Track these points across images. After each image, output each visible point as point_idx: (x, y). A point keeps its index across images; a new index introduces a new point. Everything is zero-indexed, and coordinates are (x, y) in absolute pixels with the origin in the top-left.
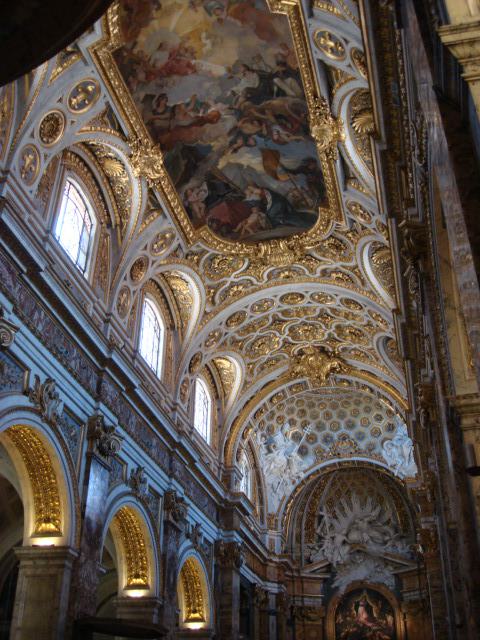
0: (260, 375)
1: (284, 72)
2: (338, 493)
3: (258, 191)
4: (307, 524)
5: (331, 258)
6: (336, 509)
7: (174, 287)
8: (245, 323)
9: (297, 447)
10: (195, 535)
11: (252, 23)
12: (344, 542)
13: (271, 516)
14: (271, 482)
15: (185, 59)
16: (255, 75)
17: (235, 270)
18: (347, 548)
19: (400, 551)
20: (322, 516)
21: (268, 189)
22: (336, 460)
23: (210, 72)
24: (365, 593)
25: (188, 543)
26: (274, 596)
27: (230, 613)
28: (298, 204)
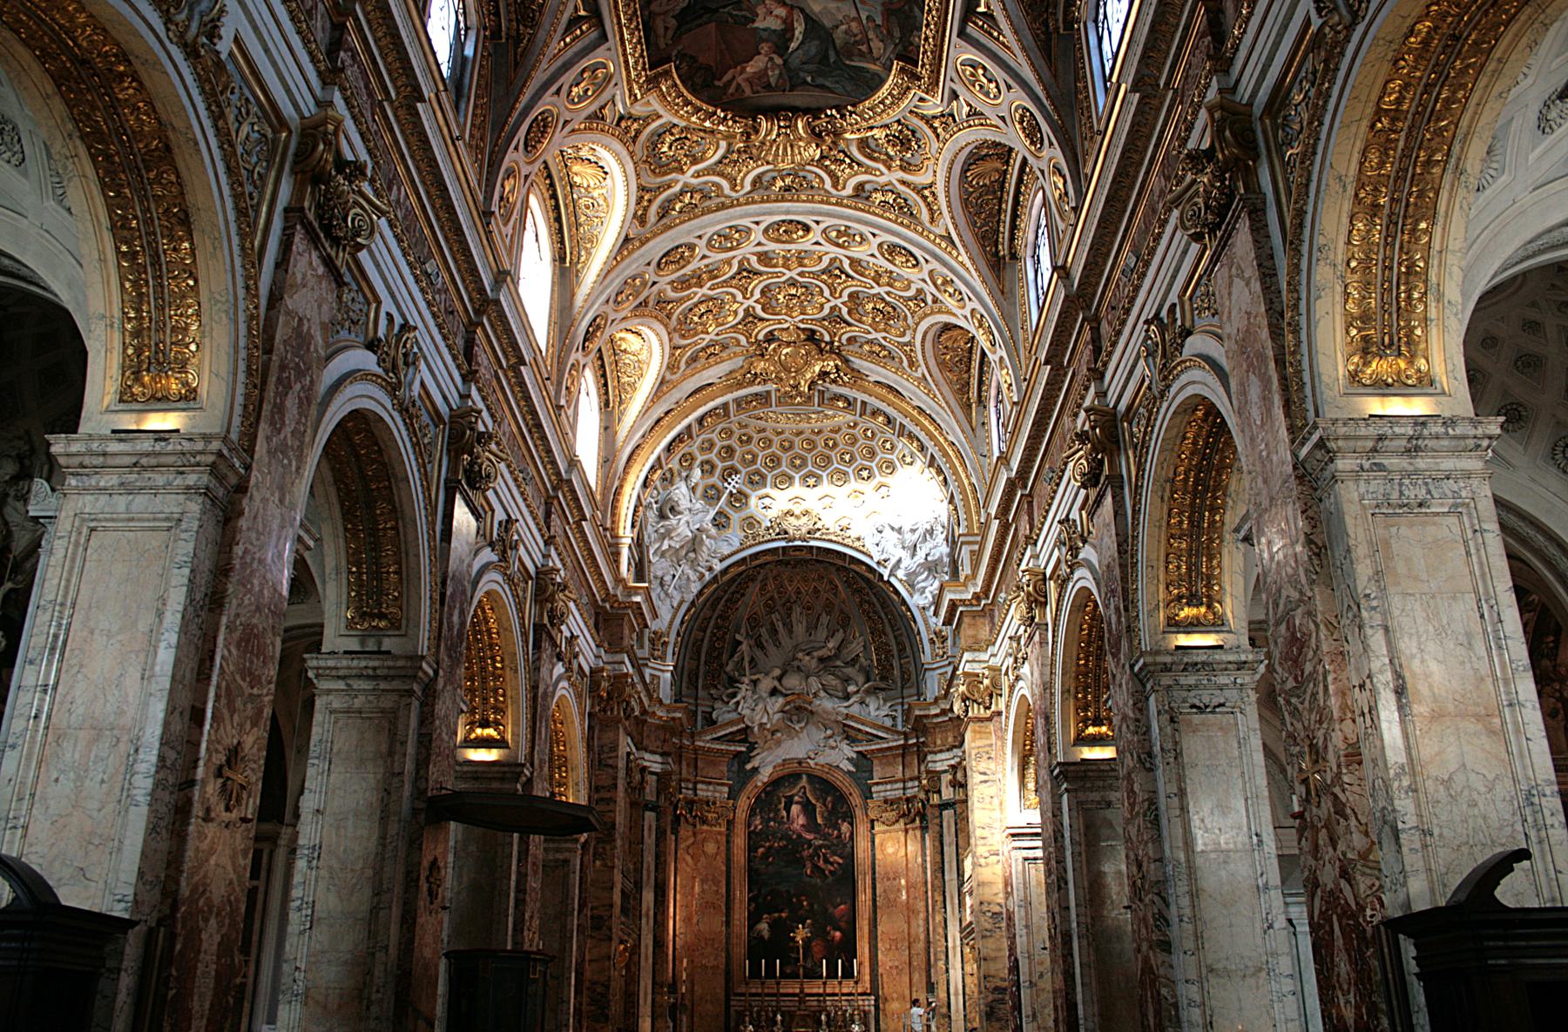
0: (688, 371)
3: (781, 12)
5: (884, 163)
6: (763, 630)
7: (577, 179)
8: (687, 270)
9: (712, 513)
10: (567, 656)
13: (657, 639)
14: (659, 574)
17: (695, 161)
18: (781, 700)
20: (740, 643)
21: (802, 10)
22: (783, 544)
24: (804, 781)
25: (559, 669)
27: (612, 800)
28: (849, 50)
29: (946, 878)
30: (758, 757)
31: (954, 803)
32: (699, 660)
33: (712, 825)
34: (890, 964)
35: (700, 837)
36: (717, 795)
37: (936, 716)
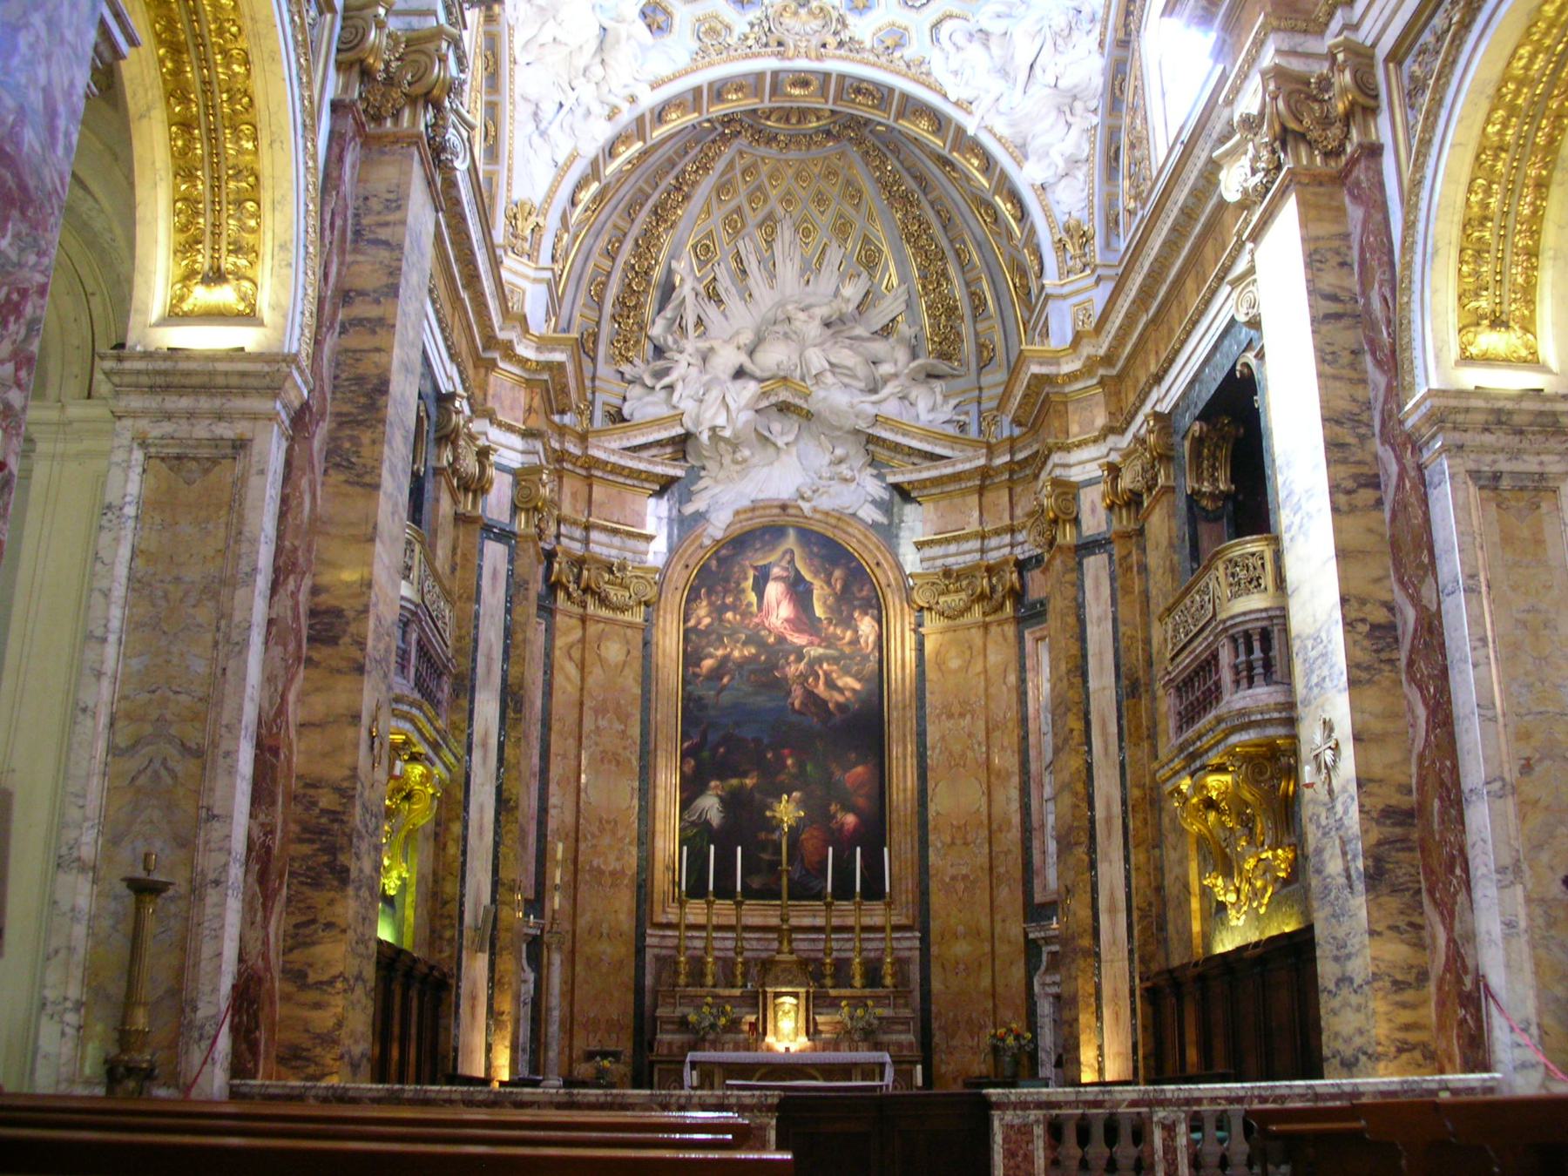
2: (734, 225)
4: (621, 302)
12: (740, 373)
14: (533, 93)
18: (752, 387)
19: (925, 417)
24: (791, 541)
26: (508, 479)
29: (1093, 684)
30: (706, 495)
31: (1109, 541)
32: (600, 305)
33: (615, 608)
34: (952, 871)
35: (593, 629)
36: (629, 555)
37: (1073, 377)
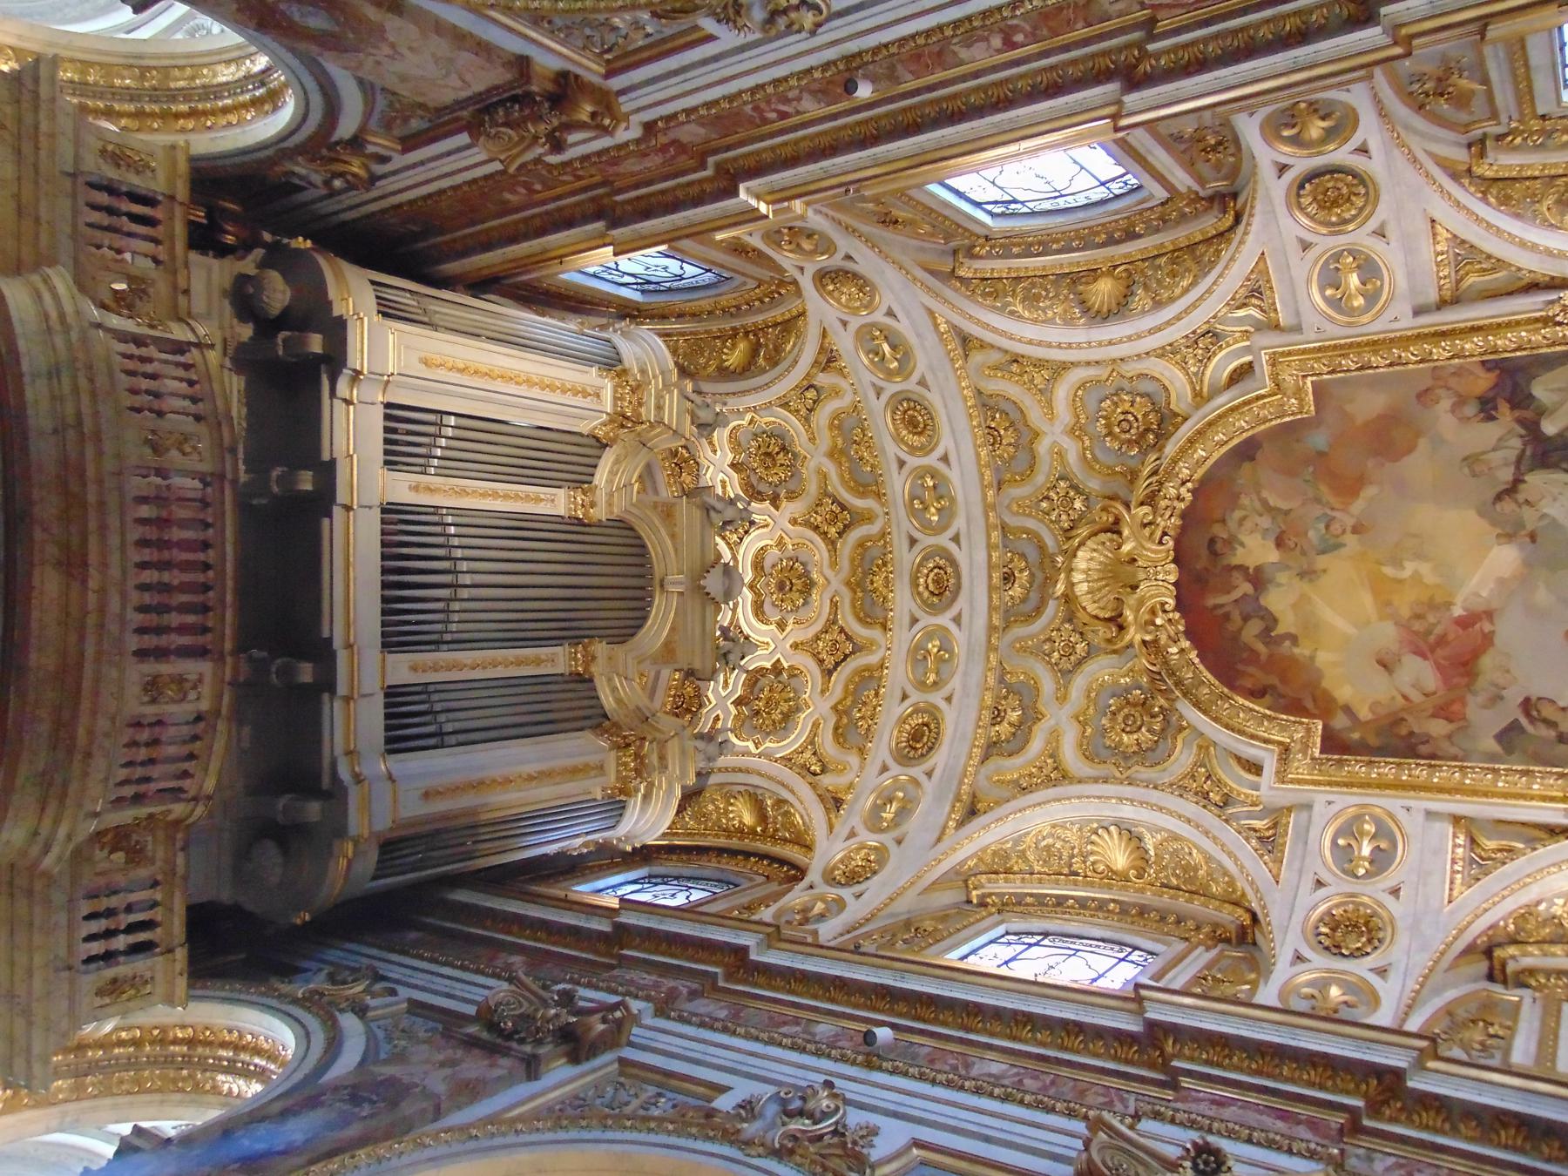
1: (1513, 408)
11: (1370, 463)
15: (1440, 624)
16: (1536, 481)
23: (1501, 581)
